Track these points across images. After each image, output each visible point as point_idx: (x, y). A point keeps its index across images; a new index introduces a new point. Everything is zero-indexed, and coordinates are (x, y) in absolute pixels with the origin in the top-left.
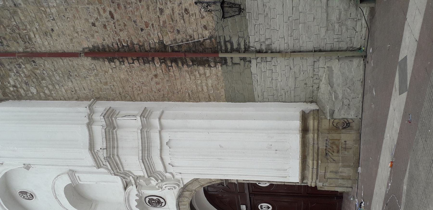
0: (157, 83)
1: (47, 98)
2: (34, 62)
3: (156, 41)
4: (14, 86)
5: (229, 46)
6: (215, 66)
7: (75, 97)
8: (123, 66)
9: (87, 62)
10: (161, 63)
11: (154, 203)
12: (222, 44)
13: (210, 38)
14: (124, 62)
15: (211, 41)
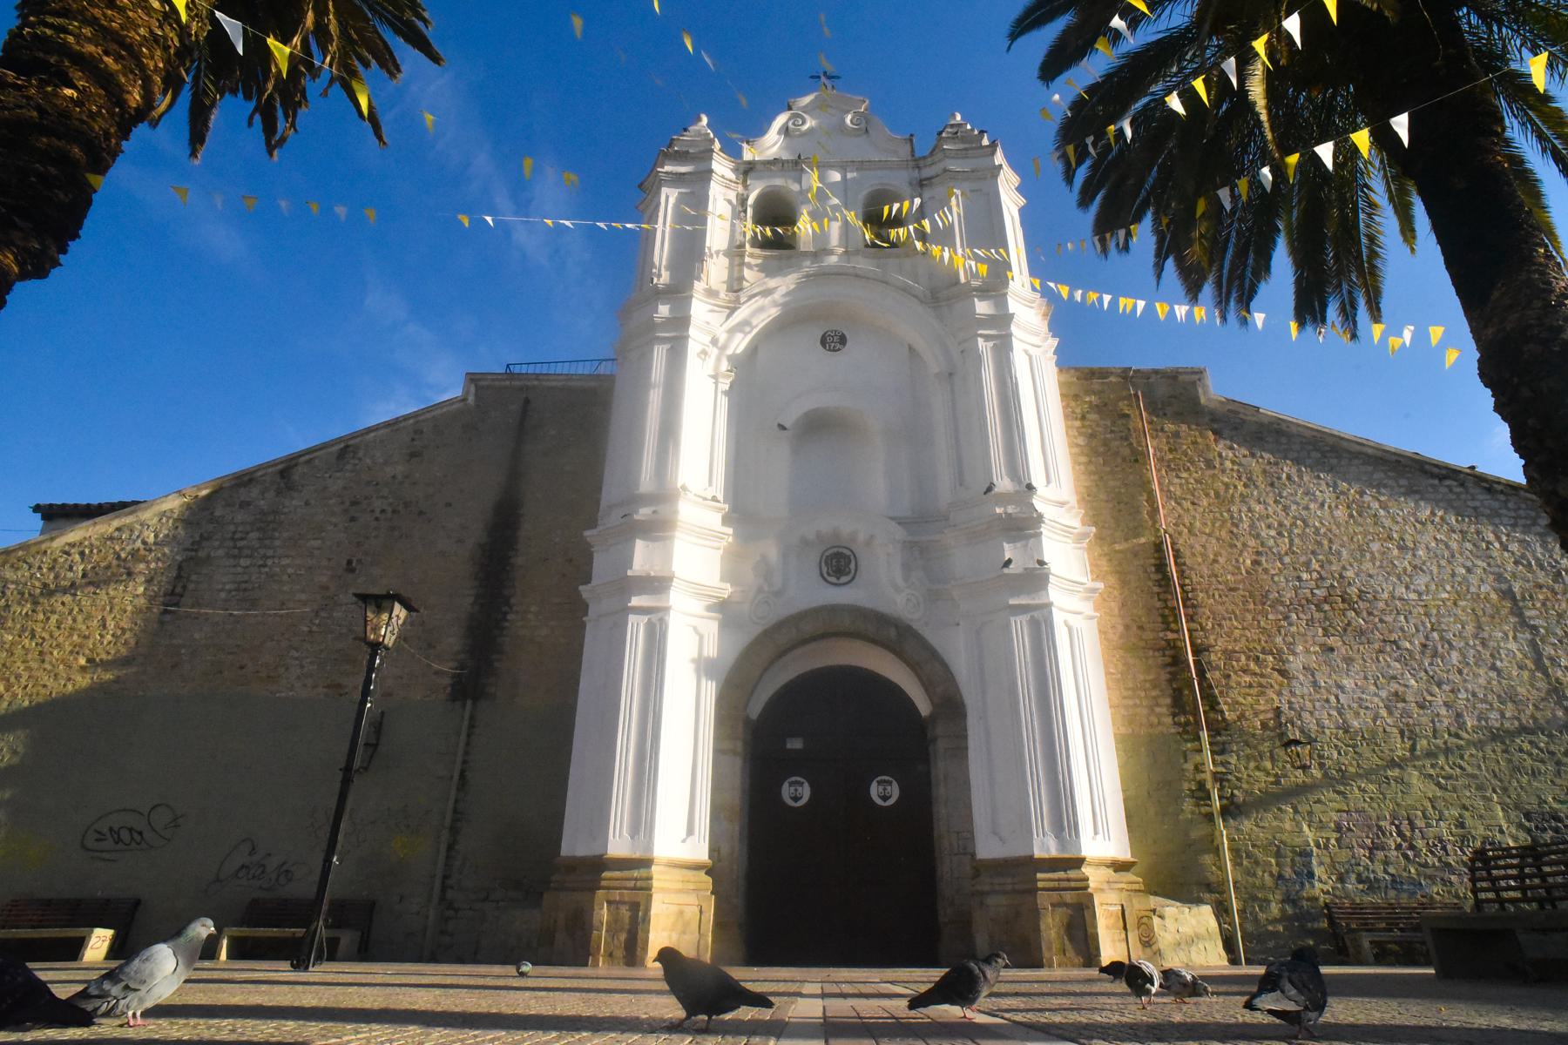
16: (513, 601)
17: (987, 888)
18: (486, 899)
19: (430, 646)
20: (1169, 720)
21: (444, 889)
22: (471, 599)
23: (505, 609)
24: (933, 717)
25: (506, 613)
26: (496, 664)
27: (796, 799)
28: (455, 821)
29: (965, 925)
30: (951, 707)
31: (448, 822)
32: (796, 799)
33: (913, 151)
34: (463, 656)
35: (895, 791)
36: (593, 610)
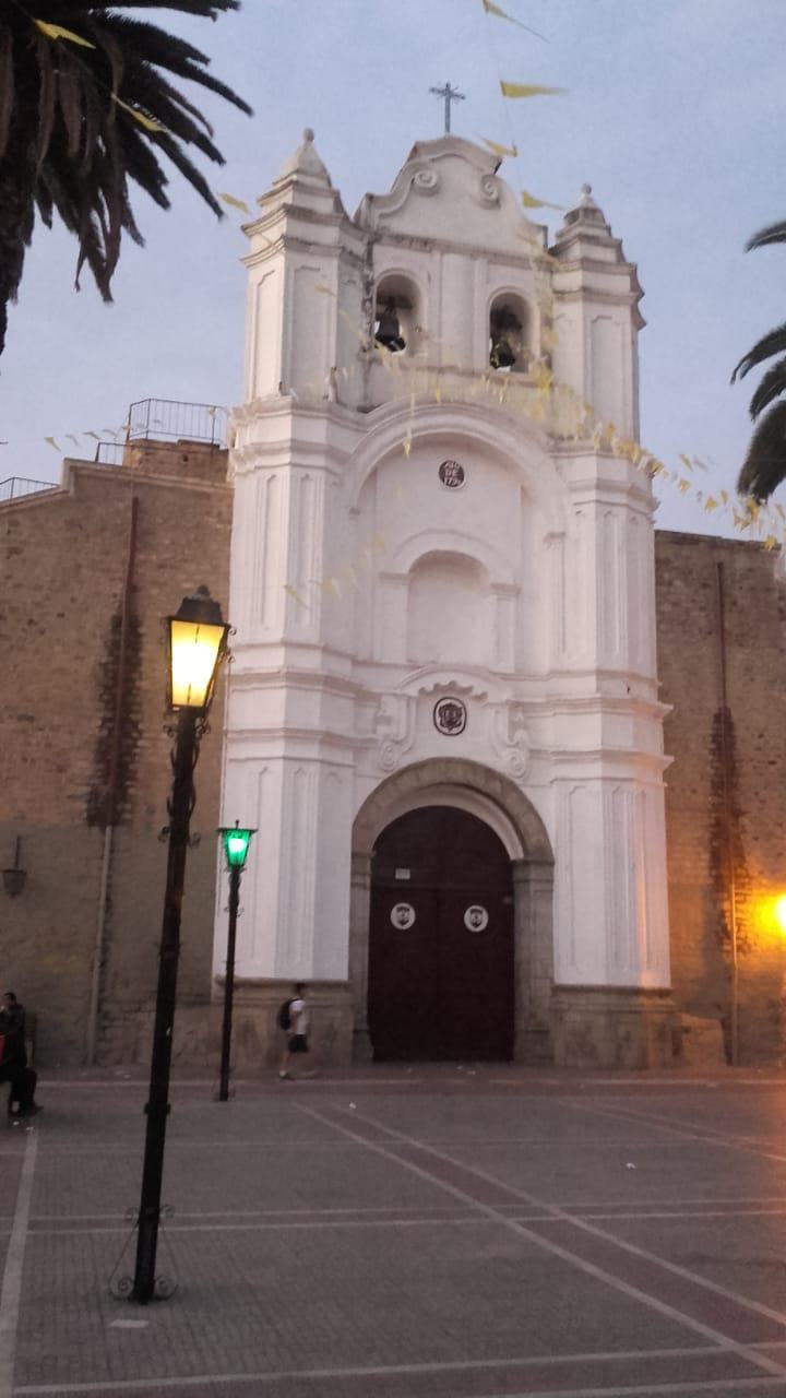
0: (683, 790)
1: (659, 622)
2: (710, 633)
3: (743, 807)
4: (670, 584)
5: (739, 898)
6: (711, 876)
7: (663, 664)
8: (706, 752)
9: (712, 705)
10: (713, 804)
11: (451, 714)
12: (744, 892)
13: (748, 876)
14: (714, 754)
15: (744, 877)
16: (141, 726)
17: (565, 1006)
18: (139, 1010)
19: (61, 769)
20: (705, 873)
21: (100, 1002)
22: (99, 723)
23: (135, 735)
24: (525, 863)
25: (136, 740)
26: (131, 791)
27: (403, 923)
28: (104, 940)
29: (543, 1033)
30: (542, 858)
31: (99, 943)
32: (403, 922)
33: (546, 245)
34: (96, 781)
35: (484, 919)
36: (233, 751)
